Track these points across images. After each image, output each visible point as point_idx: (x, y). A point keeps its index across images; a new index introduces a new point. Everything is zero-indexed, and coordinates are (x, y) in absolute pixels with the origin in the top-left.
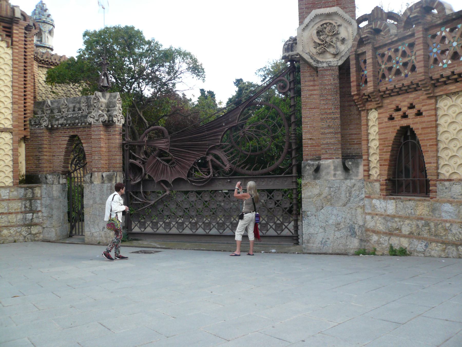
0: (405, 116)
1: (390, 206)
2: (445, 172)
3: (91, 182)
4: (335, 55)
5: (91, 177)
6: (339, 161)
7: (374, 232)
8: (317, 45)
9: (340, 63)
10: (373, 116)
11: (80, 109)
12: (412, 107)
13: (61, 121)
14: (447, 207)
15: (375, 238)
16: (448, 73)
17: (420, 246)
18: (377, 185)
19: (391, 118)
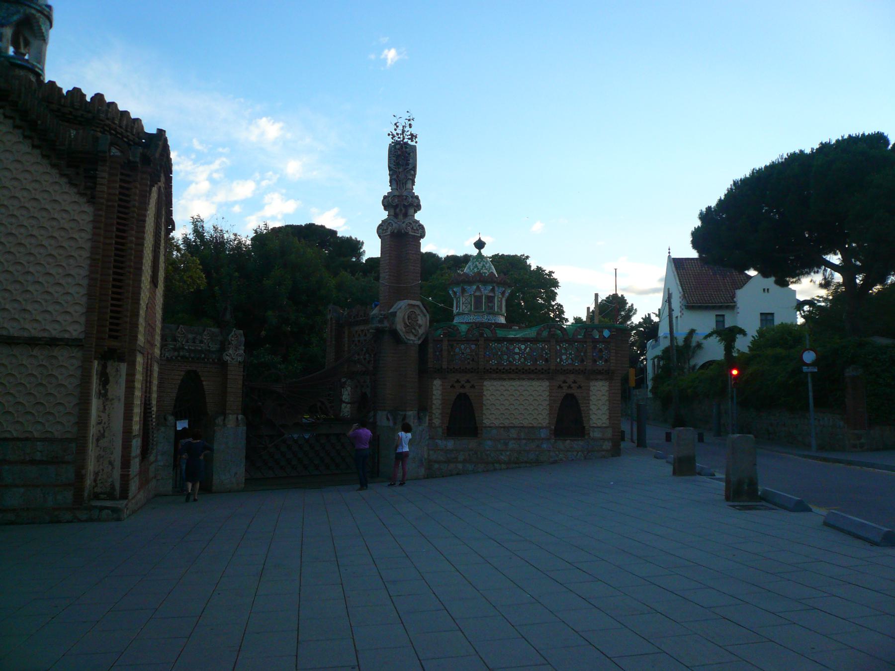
0: (463, 387)
1: (450, 444)
2: (487, 422)
3: (225, 425)
4: (415, 336)
5: (224, 420)
6: (416, 412)
7: (435, 462)
8: (406, 325)
9: (420, 342)
10: (437, 383)
11: (201, 342)
12: (468, 381)
13: (181, 353)
14: (489, 443)
15: (436, 466)
16: (495, 367)
17: (470, 467)
18: (440, 430)
19: (453, 386)
